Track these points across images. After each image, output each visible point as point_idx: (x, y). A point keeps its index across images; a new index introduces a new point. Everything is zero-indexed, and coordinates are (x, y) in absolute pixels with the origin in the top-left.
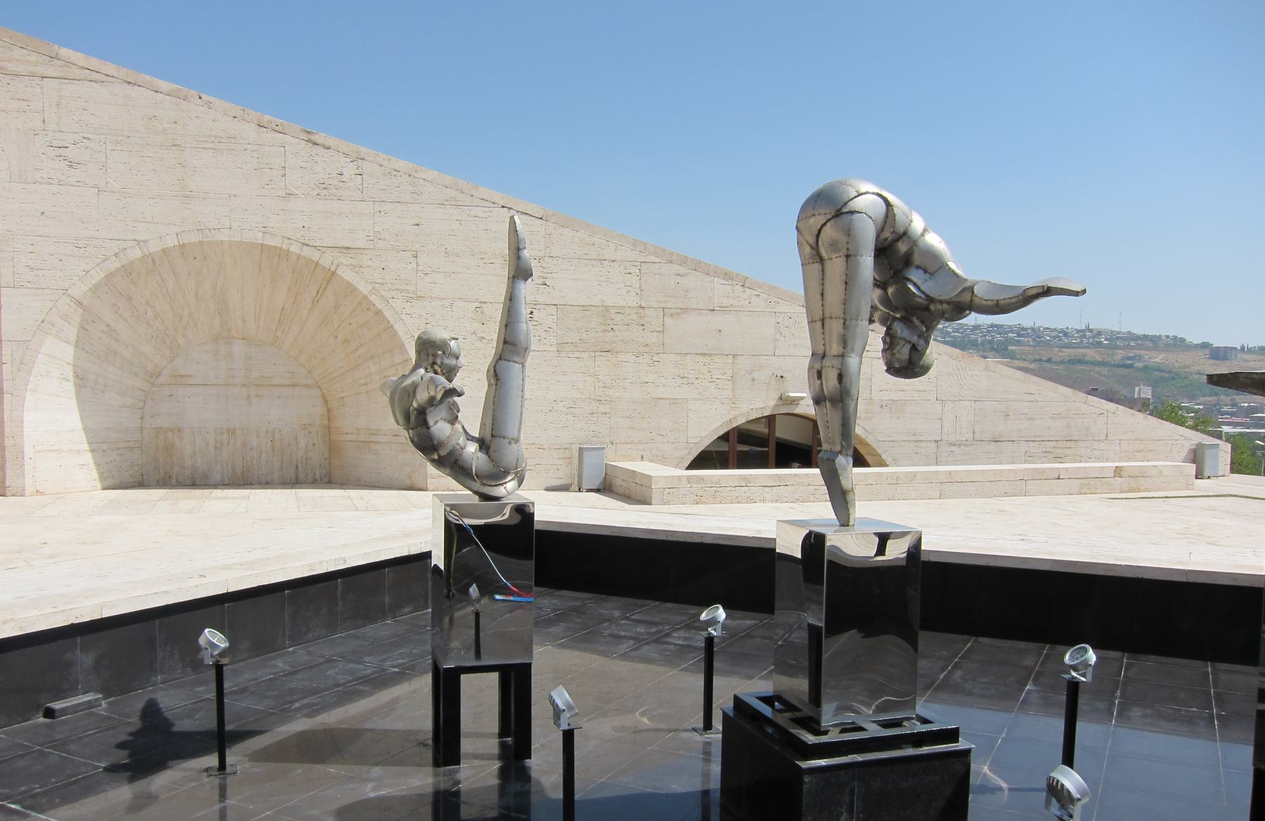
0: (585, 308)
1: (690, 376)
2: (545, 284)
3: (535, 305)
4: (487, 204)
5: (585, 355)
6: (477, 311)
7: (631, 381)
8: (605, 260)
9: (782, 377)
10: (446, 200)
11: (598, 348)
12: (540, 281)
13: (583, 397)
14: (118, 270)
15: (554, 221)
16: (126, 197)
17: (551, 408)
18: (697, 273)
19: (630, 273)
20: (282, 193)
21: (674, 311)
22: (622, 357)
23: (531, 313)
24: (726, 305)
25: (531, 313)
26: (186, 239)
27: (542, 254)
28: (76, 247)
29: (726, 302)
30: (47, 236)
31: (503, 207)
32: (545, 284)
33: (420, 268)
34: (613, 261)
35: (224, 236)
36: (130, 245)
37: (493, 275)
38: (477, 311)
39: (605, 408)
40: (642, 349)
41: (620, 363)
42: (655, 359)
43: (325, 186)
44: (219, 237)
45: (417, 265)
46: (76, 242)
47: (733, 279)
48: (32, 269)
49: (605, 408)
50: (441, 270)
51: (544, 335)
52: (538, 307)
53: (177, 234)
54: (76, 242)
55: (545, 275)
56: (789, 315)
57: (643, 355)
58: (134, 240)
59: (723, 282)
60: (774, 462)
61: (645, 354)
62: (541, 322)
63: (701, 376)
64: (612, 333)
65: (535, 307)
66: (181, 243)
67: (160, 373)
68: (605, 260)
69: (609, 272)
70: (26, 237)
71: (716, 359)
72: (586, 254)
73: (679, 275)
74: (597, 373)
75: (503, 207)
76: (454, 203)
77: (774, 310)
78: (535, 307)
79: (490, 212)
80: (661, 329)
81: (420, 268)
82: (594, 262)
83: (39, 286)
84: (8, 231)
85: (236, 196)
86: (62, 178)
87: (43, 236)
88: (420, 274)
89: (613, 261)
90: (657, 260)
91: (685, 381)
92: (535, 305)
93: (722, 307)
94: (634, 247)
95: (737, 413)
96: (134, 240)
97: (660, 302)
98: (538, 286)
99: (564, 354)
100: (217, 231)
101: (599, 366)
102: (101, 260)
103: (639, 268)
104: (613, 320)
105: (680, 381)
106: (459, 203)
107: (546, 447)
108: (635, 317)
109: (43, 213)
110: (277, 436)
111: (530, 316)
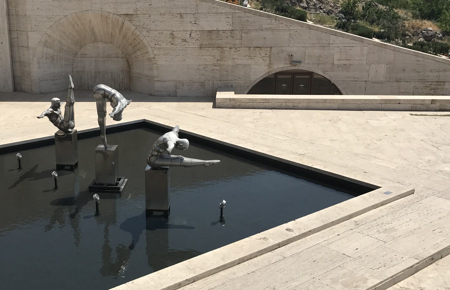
0: (210, 32)
12: (194, 22)
19: (228, 18)
33: (151, 20)
34: (222, 13)
45: (151, 19)
47: (271, 17)
50: (159, 20)
51: (195, 42)
52: (193, 32)
63: (257, 56)
81: (151, 20)
88: (151, 22)
89: (222, 13)
92: (192, 31)
95: (272, 69)
105: (247, 57)
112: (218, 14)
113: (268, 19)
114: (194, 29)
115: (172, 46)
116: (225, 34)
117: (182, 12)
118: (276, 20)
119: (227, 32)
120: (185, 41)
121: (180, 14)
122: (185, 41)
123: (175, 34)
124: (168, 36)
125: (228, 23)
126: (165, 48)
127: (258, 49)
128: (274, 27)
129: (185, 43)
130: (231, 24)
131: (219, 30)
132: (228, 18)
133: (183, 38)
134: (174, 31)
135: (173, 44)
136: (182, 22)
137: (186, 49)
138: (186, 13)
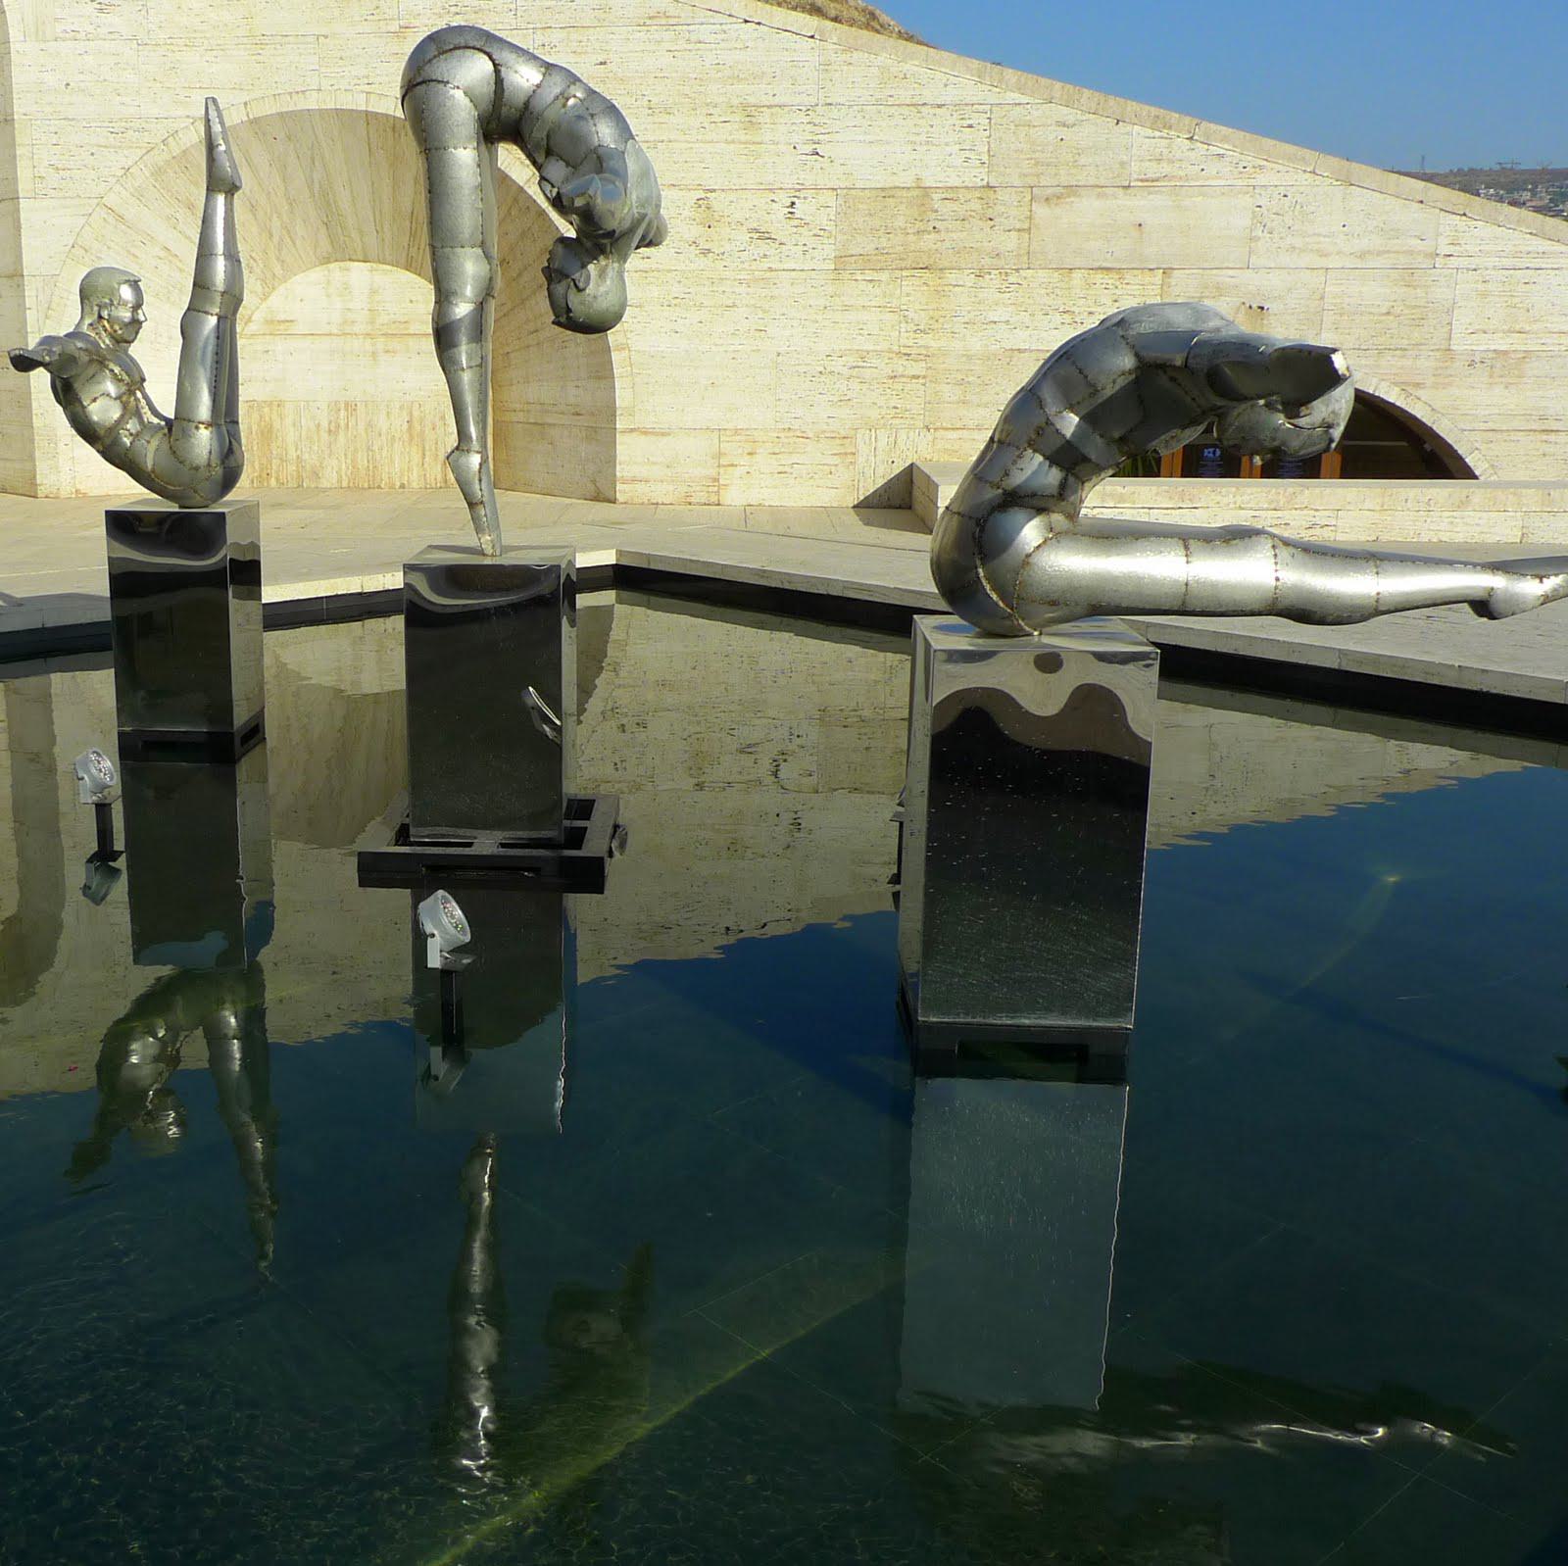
0: (886, 193)
1: (1077, 310)
2: (817, 154)
3: (799, 190)
4: (719, 18)
5: (884, 276)
6: (700, 206)
7: (966, 319)
8: (925, 104)
9: (1262, 308)
10: (650, 18)
11: (908, 263)
12: (809, 148)
13: (878, 348)
14: (167, 162)
15: (835, 40)
16: (174, 52)
17: (822, 369)
18: (1100, 120)
19: (970, 126)
20: (394, 27)
21: (1050, 191)
22: (951, 277)
23: (793, 203)
24: (1154, 176)
25: (793, 203)
26: (257, 111)
27: (813, 101)
28: (112, 133)
29: (1153, 170)
30: (73, 119)
31: (746, 21)
32: (817, 154)
34: (939, 106)
35: (312, 102)
36: (183, 125)
37: (727, 142)
38: (700, 206)
39: (918, 368)
40: (987, 261)
41: (946, 288)
42: (1012, 279)
43: (458, 10)
44: (302, 104)
46: (111, 125)
47: (1170, 128)
48: (57, 169)
49: (918, 368)
51: (811, 242)
52: (802, 194)
53: (246, 104)
54: (111, 125)
55: (816, 138)
56: (1282, 190)
57: (990, 273)
58: (188, 117)
59: (1149, 132)
60: (1179, 471)
61: (994, 272)
62: (808, 219)
64: (933, 236)
65: (797, 194)
66: (251, 117)
67: (250, 318)
68: (925, 104)
69: (932, 126)
70: (48, 122)
71: (1129, 277)
72: (890, 96)
73: (1064, 125)
74: (905, 307)
75: (746, 21)
76: (663, 22)
77: (1252, 182)
78: (797, 194)
79: (725, 32)
80: (1026, 226)
82: (905, 110)
83: (67, 195)
84: (25, 115)
85: (326, 37)
86: (90, 29)
87: (69, 119)
89: (939, 106)
90: (1024, 99)
91: (1067, 318)
92: (799, 190)
93: (1147, 181)
94: (979, 77)
96: (188, 117)
97: (1025, 175)
98: (804, 157)
99: (846, 275)
100: (300, 95)
101: (908, 295)
102: (144, 151)
103: (988, 116)
104: (936, 211)
105: (1058, 318)
106: (672, 21)
107: (810, 435)
108: (976, 205)
109: (68, 85)
110: (416, 414)
111: (791, 210)
112: (923, 109)
113: (1157, 134)
114: (809, 179)
115: (702, 262)
116: (955, 206)
117: (752, 100)
118: (1191, 138)
119: (962, 195)
120: (765, 236)
121: (745, 106)
122: (765, 236)
123: (715, 204)
124: (686, 213)
125: (967, 154)
126: (669, 271)
127: (1109, 279)
128: (1181, 173)
129: (764, 247)
130: (985, 158)
131: (928, 185)
132: (970, 126)
133: (755, 225)
134: (714, 191)
135: (706, 252)
136: (753, 147)
137: (768, 274)
138: (776, 101)
